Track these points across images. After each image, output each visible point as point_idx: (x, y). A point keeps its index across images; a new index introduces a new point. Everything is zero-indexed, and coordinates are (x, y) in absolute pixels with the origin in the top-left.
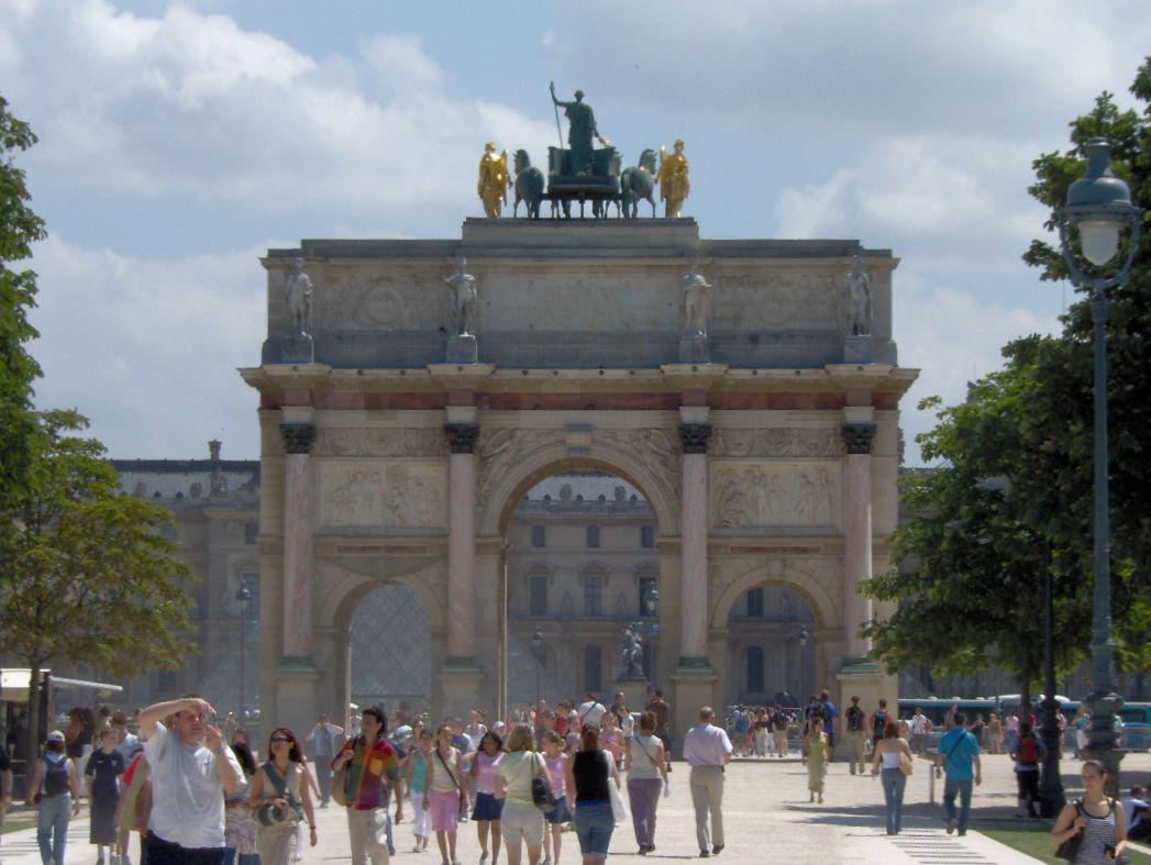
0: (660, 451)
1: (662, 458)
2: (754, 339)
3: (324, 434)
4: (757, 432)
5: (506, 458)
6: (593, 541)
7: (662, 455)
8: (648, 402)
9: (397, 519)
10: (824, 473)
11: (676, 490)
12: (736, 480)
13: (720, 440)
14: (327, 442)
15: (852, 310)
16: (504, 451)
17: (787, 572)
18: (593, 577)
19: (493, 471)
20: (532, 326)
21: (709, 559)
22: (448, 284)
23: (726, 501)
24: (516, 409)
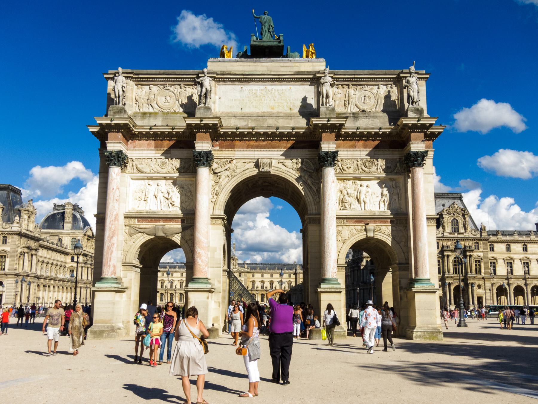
0: (308, 170)
1: (309, 174)
2: (355, 116)
3: (133, 161)
4: (359, 160)
5: (227, 173)
6: (262, 276)
7: (309, 172)
8: (302, 145)
9: (170, 205)
10: (394, 183)
11: (317, 190)
12: (348, 186)
13: (339, 163)
14: (134, 164)
15: (412, 94)
16: (226, 170)
17: (377, 233)
18: (263, 282)
19: (221, 180)
20: (242, 109)
21: (337, 226)
22: (198, 83)
23: (344, 196)
24: (234, 148)
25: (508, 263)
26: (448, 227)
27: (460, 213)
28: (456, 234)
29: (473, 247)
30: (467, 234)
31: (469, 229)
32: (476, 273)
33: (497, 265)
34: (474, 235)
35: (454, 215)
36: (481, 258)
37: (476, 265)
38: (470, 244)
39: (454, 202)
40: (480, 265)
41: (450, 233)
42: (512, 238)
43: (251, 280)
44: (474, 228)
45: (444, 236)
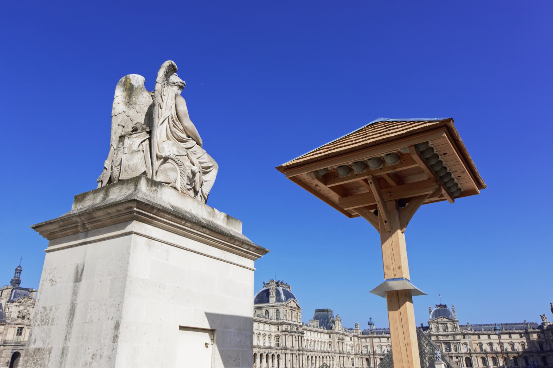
43: (477, 342)
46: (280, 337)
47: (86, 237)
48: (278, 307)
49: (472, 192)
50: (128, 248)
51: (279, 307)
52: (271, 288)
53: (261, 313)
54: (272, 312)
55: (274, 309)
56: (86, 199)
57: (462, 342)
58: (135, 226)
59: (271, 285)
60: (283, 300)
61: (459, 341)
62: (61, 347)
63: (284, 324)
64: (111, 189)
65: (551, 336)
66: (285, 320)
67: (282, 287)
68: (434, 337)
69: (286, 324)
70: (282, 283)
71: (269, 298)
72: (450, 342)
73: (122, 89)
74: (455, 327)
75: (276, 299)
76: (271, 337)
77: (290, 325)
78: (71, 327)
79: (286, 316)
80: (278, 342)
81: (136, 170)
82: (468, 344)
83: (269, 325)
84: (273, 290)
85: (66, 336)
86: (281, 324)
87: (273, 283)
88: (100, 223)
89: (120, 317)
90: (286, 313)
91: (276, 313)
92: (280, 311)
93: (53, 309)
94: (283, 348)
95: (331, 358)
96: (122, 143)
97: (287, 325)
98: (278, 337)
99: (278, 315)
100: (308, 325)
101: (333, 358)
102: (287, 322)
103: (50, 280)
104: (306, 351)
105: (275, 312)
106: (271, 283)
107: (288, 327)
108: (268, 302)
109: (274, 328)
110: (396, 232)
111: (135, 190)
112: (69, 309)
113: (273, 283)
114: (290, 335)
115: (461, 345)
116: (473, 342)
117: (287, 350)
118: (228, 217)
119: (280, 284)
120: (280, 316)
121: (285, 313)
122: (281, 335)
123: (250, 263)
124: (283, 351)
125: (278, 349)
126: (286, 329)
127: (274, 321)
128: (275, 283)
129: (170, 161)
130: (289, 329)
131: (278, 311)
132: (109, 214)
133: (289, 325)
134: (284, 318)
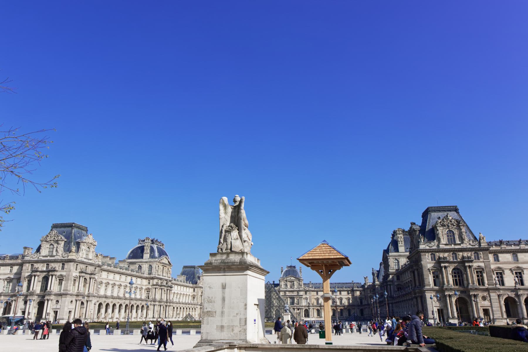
25: (516, 273)
26: (443, 239)
27: (455, 224)
28: (453, 245)
29: (473, 257)
30: (464, 245)
31: (467, 240)
32: (479, 284)
33: (504, 276)
34: (472, 246)
35: (448, 226)
36: (483, 269)
37: (478, 276)
38: (469, 255)
39: (448, 214)
40: (482, 276)
41: (446, 245)
42: (518, 248)
43: (316, 297)
44: (472, 238)
45: (440, 248)
46: (151, 290)
47: (225, 273)
48: (151, 263)
49: (348, 265)
50: (246, 280)
51: (152, 263)
52: (146, 246)
53: (135, 268)
54: (145, 267)
55: (147, 265)
56: (217, 256)
57: (304, 297)
58: (249, 272)
59: (146, 243)
60: (156, 257)
61: (302, 297)
62: (221, 311)
63: (156, 278)
64: (230, 255)
65: (369, 293)
66: (156, 275)
67: (156, 244)
68: (283, 292)
69: (157, 279)
70: (157, 241)
71: (143, 254)
72: (295, 297)
73: (222, 206)
74: (300, 285)
75: (150, 256)
76: (141, 290)
77: (161, 280)
78: (224, 304)
79: (158, 271)
80: (148, 295)
81: (238, 247)
82: (308, 299)
83: (141, 279)
84: (147, 248)
85: (222, 307)
86: (153, 278)
87: (149, 241)
88: (233, 269)
89: (247, 302)
90: (158, 268)
91: (149, 268)
92: (153, 267)
93: (213, 298)
94: (153, 300)
95: (194, 309)
96: (230, 235)
97: (158, 280)
98: (148, 290)
99: (150, 270)
100: (176, 279)
101: (195, 309)
102: (159, 276)
103: (209, 287)
104: (173, 303)
105: (147, 268)
106: (147, 241)
107: (159, 281)
108: (142, 257)
109: (145, 282)
110: (327, 281)
111: (243, 257)
112: (222, 298)
113: (149, 241)
114: (160, 289)
115: (303, 299)
116: (312, 297)
117: (156, 302)
118: (258, 259)
119: (155, 242)
120: (152, 272)
121: (157, 269)
122: (151, 289)
123: (263, 277)
124: (153, 303)
125: (148, 301)
126: (157, 283)
127: (146, 275)
128: (150, 241)
129: (246, 242)
130: (160, 283)
131: (151, 267)
132: (237, 267)
133: (160, 279)
134: (156, 273)
